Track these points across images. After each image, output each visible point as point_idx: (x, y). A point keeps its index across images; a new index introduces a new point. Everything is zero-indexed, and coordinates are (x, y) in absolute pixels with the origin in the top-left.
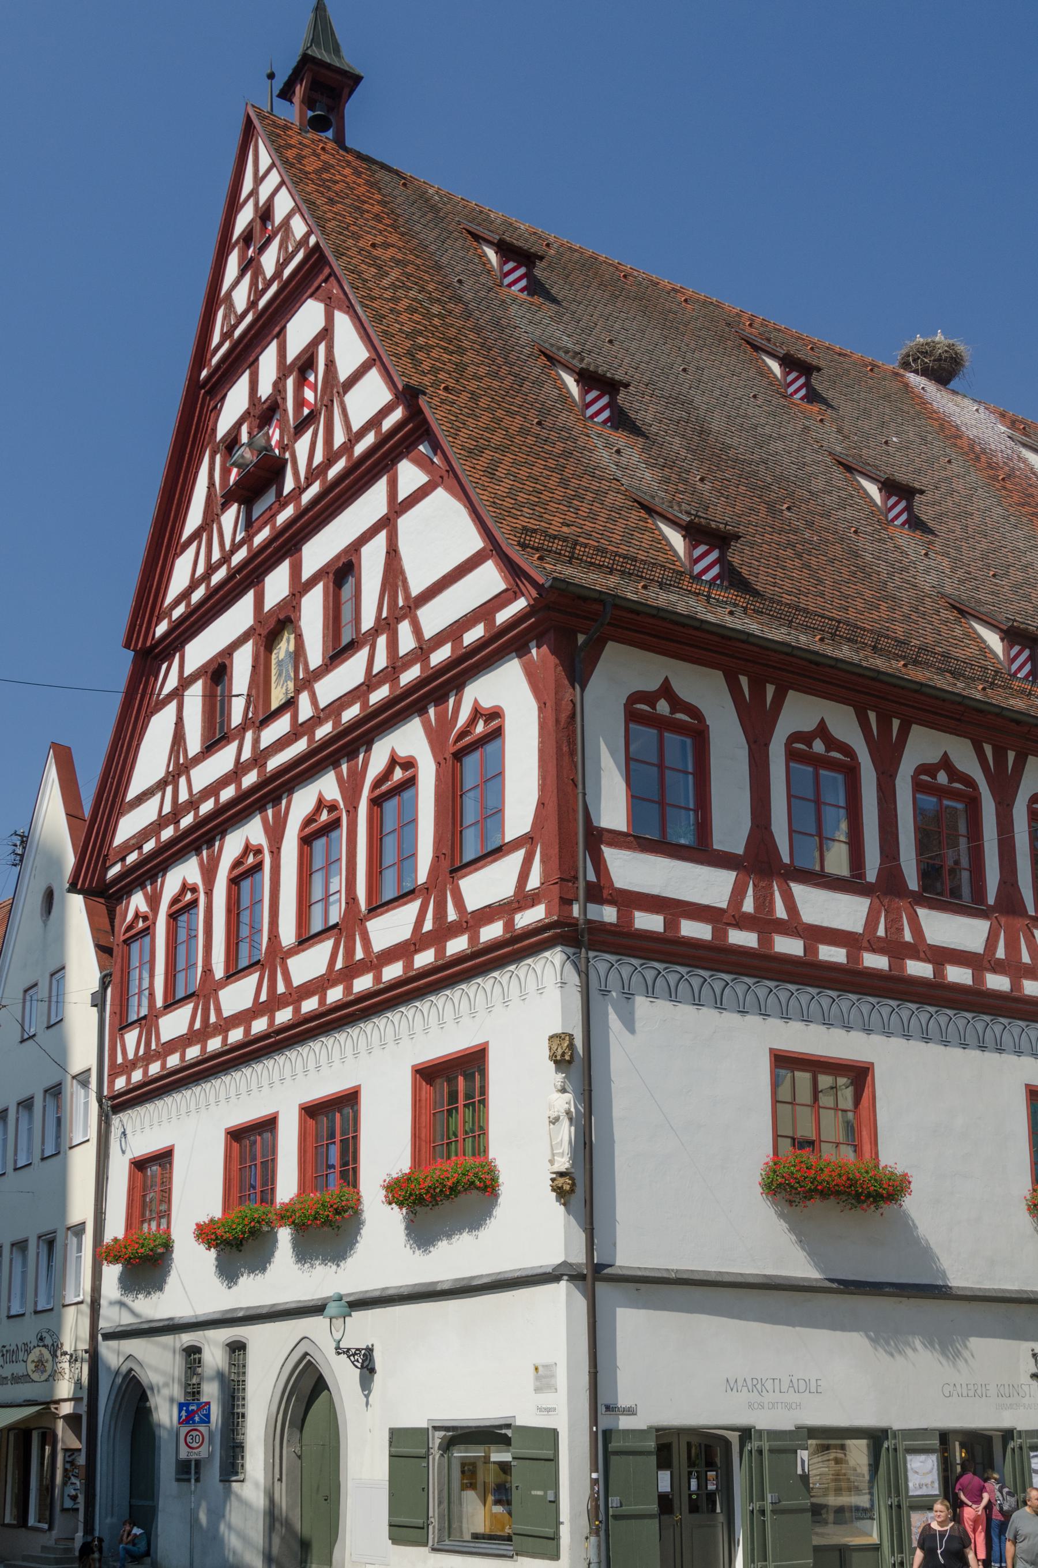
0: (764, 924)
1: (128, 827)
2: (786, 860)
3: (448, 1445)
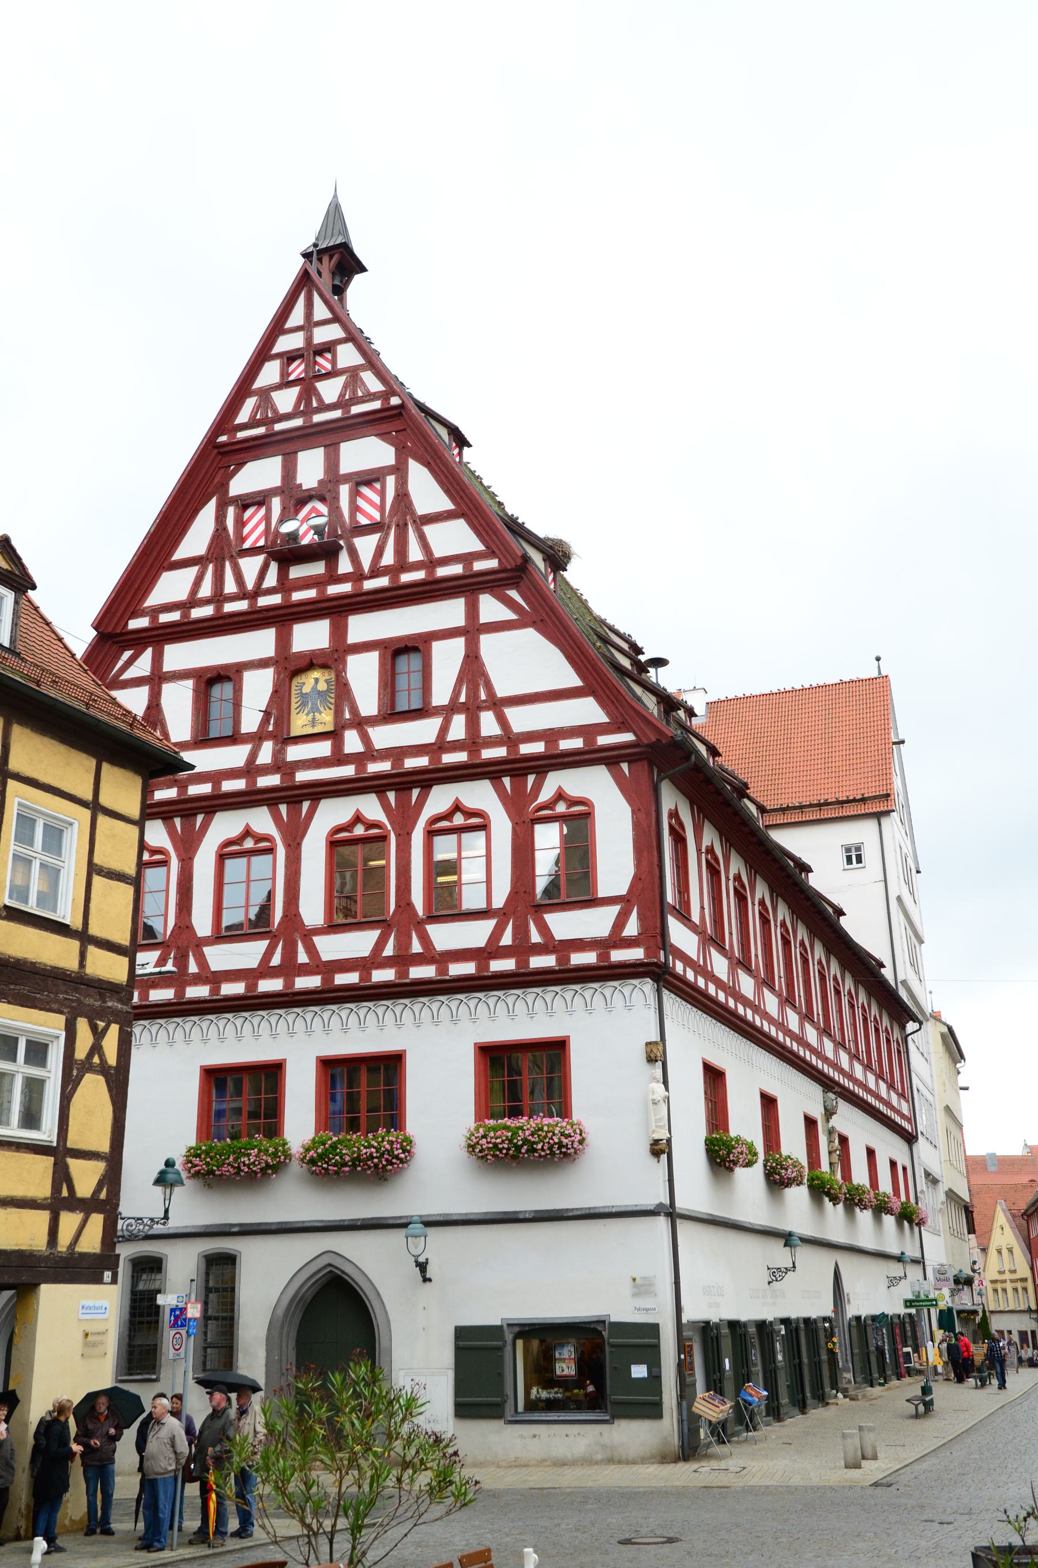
3: (518, 1336)
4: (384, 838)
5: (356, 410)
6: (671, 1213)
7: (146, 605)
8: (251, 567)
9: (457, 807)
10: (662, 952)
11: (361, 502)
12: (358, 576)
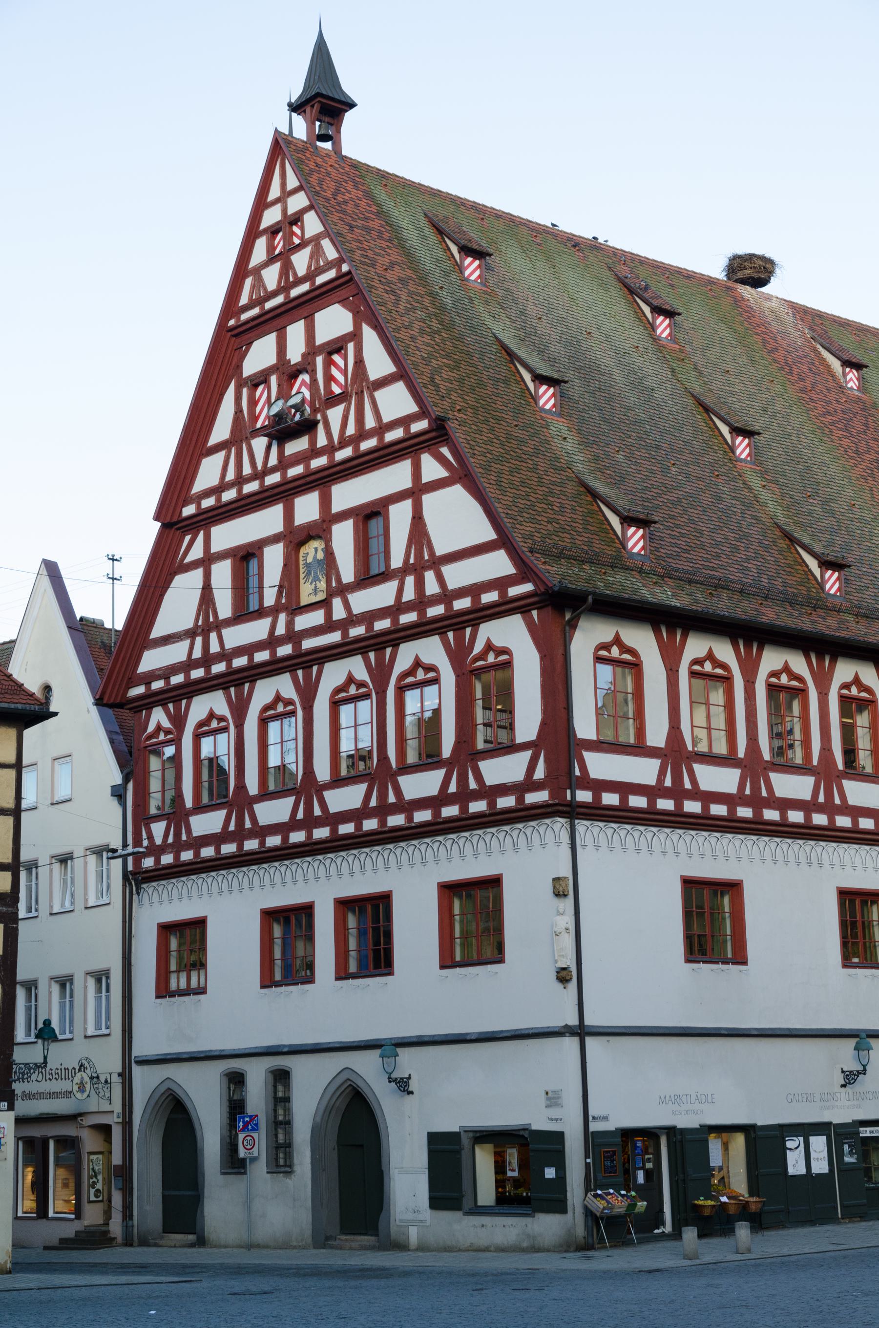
0: (678, 793)
1: (151, 660)
2: (690, 748)
5: (295, 292)
6: (581, 1032)
7: (193, 492)
8: (259, 444)
10: (568, 792)
11: (334, 372)
12: (330, 449)
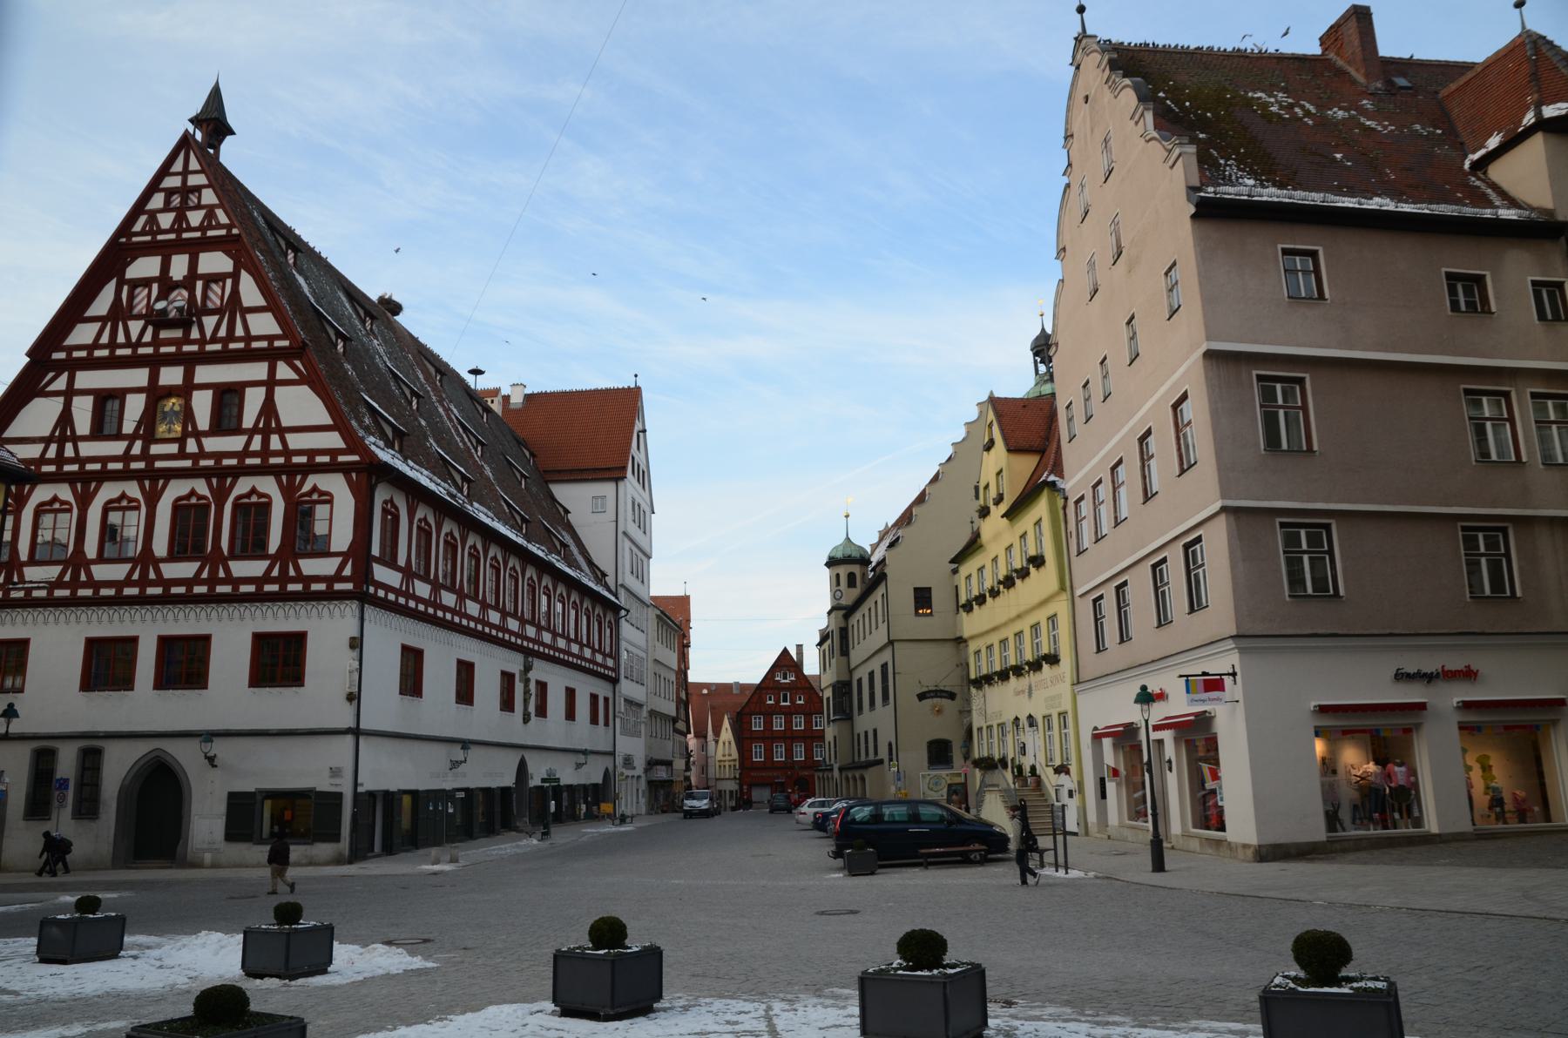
4: (208, 506)
6: (356, 732)
9: (253, 491)
12: (202, 341)
